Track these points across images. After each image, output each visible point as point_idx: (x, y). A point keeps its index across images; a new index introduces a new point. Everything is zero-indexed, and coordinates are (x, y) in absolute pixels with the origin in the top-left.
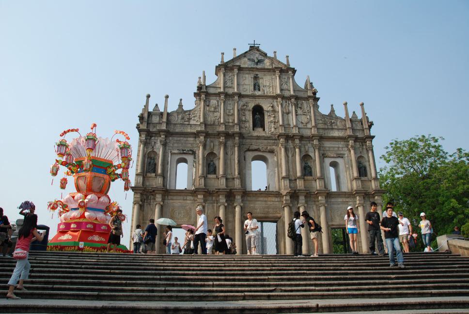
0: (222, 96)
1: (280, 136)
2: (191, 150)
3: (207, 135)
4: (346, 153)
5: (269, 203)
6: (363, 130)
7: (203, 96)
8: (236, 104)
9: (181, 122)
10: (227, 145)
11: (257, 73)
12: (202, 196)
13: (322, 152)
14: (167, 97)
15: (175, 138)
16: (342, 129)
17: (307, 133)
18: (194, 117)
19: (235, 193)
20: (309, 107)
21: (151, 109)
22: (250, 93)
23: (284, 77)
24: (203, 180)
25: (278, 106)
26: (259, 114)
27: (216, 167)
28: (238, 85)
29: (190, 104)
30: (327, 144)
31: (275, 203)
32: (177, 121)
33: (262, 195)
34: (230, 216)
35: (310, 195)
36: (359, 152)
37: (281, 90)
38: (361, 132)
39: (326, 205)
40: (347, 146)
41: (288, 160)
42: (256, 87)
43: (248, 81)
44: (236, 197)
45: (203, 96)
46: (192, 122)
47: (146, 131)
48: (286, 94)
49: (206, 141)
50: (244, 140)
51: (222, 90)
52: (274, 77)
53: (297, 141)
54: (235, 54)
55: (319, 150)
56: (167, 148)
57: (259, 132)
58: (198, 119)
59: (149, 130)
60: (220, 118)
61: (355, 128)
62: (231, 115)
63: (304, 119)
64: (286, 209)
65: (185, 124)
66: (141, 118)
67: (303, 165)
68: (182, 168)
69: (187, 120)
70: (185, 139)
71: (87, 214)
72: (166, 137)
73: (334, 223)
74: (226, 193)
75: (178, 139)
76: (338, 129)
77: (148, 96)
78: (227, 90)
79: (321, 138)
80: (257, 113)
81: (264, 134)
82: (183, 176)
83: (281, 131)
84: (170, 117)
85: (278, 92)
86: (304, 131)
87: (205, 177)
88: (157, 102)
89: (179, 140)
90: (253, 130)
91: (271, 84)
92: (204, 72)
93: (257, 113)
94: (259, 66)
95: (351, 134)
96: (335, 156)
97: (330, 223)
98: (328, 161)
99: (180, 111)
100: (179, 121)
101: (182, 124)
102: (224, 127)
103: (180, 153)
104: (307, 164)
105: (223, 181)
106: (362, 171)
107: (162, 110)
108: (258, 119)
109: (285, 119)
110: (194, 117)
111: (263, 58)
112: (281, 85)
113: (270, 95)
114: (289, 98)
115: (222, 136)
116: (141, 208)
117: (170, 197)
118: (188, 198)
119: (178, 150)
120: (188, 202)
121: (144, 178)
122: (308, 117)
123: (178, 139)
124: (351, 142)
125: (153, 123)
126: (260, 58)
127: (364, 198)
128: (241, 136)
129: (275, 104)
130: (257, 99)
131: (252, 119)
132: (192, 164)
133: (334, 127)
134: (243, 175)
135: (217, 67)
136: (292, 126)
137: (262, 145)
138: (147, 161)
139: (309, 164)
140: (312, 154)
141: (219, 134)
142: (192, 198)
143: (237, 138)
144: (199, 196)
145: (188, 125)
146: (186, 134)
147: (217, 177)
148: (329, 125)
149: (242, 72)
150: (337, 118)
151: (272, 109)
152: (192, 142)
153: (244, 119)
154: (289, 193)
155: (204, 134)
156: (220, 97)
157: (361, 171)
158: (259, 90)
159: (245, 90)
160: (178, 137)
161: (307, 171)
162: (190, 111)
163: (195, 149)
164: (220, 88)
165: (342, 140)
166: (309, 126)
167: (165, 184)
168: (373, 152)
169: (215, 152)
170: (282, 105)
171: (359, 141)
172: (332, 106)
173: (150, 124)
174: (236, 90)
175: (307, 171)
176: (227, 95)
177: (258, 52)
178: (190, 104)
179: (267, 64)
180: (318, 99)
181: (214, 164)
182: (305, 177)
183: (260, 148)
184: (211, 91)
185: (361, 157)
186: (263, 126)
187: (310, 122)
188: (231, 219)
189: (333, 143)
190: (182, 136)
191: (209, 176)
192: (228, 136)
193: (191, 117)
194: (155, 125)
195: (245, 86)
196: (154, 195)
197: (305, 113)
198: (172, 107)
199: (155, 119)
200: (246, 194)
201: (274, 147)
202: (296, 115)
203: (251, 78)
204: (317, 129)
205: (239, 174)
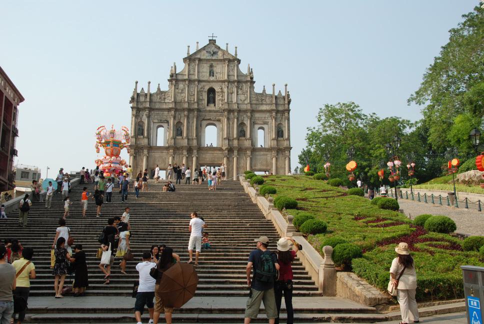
3: (176, 110)
4: (270, 121)
7: (174, 82)
11: (212, 62)
14: (149, 83)
17: (243, 107)
21: (139, 91)
24: (173, 140)
28: (198, 72)
29: (165, 87)
30: (257, 115)
34: (190, 163)
35: (241, 150)
36: (279, 121)
37: (228, 76)
38: (283, 106)
40: (271, 116)
41: (229, 127)
42: (212, 73)
43: (205, 68)
46: (166, 101)
48: (232, 79)
49: (175, 114)
50: (201, 113)
51: (186, 77)
53: (236, 114)
54: (197, 47)
55: (251, 119)
56: (150, 119)
57: (211, 107)
63: (242, 97)
64: (225, 159)
66: (133, 98)
67: (240, 129)
68: (161, 131)
71: (112, 165)
73: (256, 168)
76: (266, 104)
77: (137, 83)
79: (253, 111)
81: (214, 109)
82: (162, 137)
83: (226, 107)
84: (152, 97)
85: (226, 78)
87: (174, 138)
88: (143, 86)
90: (208, 105)
91: (221, 72)
92: (175, 63)
94: (214, 58)
95: (275, 108)
97: (254, 168)
98: (257, 126)
102: (187, 104)
103: (159, 122)
106: (280, 133)
107: (146, 92)
109: (230, 97)
111: (217, 50)
112: (228, 72)
114: (234, 82)
117: (153, 151)
118: (164, 151)
120: (164, 154)
121: (136, 138)
123: (158, 112)
124: (274, 114)
126: (216, 50)
128: (199, 110)
129: (223, 86)
134: (199, 137)
137: (212, 116)
139: (244, 129)
141: (184, 110)
142: (166, 152)
143: (196, 112)
144: (171, 151)
150: (267, 95)
152: (166, 115)
153: (201, 98)
158: (213, 76)
161: (242, 133)
162: (166, 92)
163: (168, 119)
164: (185, 75)
166: (246, 102)
170: (228, 87)
174: (196, 77)
175: (242, 133)
177: (214, 46)
178: (165, 87)
179: (220, 55)
180: (254, 82)
184: (180, 77)
185: (280, 124)
186: (214, 102)
188: (190, 165)
191: (178, 137)
192: (190, 110)
196: (143, 150)
198: (153, 90)
199: (142, 99)
200: (200, 149)
201: (221, 117)
202: (237, 94)
205: (197, 136)
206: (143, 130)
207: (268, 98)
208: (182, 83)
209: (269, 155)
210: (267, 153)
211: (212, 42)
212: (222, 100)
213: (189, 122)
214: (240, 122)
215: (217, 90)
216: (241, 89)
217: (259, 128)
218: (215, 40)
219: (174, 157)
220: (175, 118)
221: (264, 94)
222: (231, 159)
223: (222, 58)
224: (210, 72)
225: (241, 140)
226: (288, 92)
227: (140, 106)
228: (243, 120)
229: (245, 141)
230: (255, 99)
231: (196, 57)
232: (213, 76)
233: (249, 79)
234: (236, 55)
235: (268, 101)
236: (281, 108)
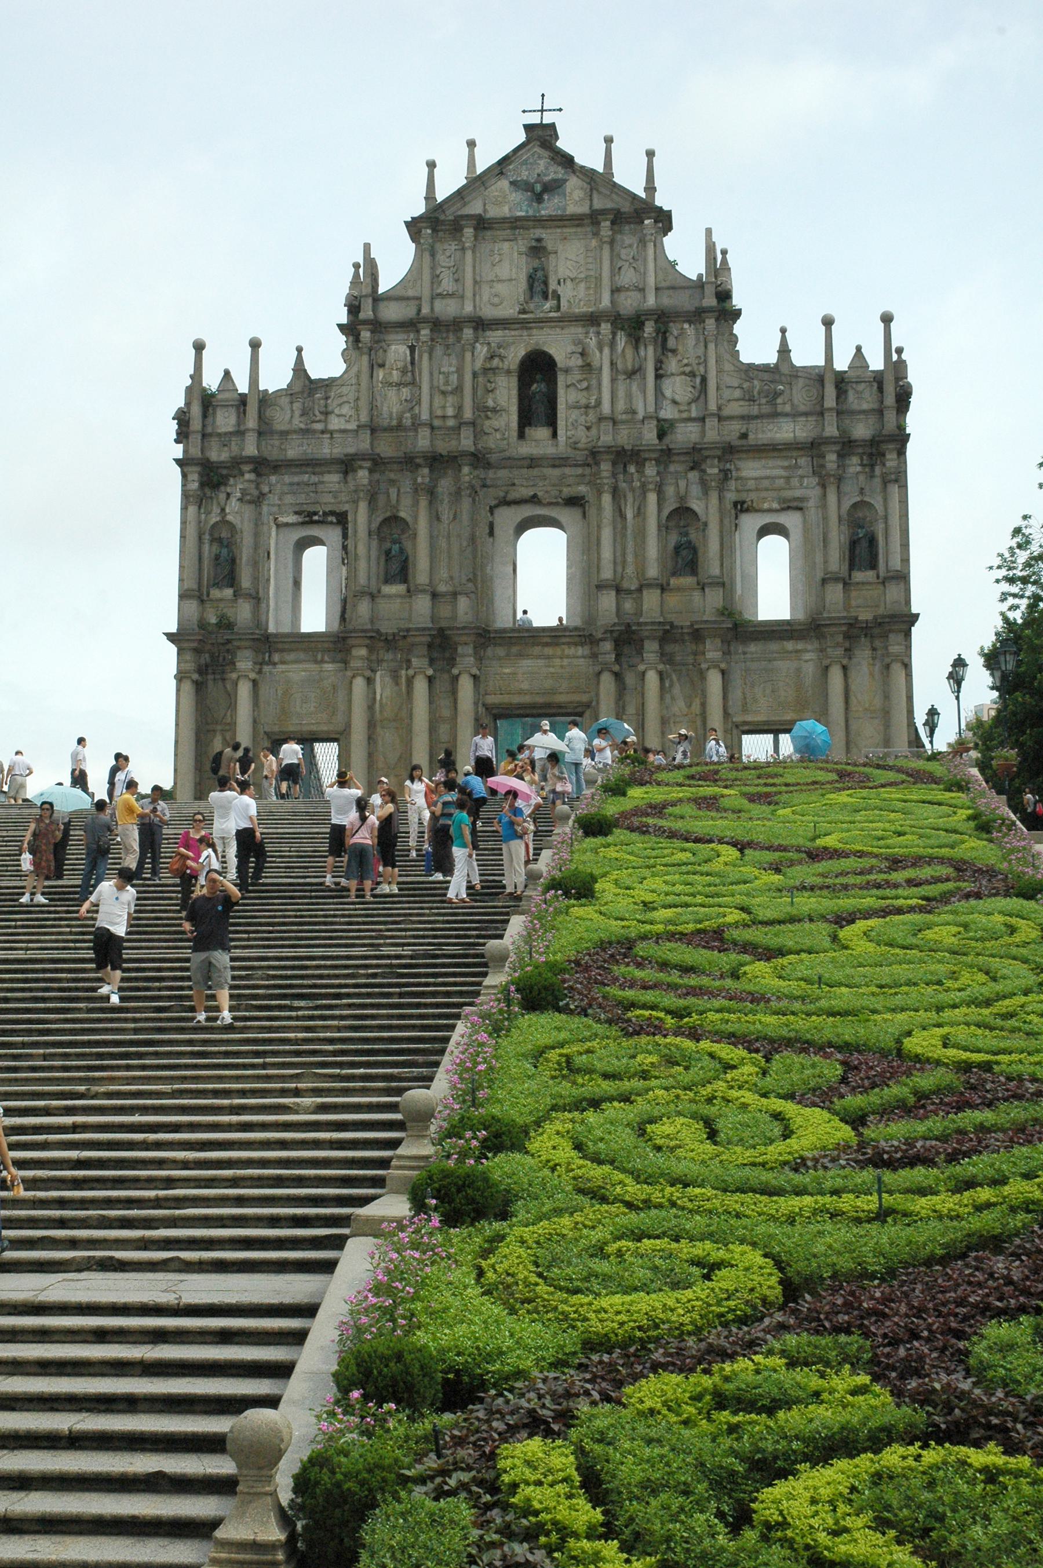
1: (594, 455)
2: (332, 513)
4: (815, 493)
5: (557, 662)
6: (880, 412)
8: (468, 355)
9: (302, 426)
10: (440, 490)
11: (539, 233)
12: (363, 652)
13: (731, 496)
14: (255, 345)
15: (287, 479)
16: (806, 414)
18: (340, 405)
19: (457, 639)
20: (702, 344)
23: (627, 242)
25: (601, 351)
26: (543, 380)
27: (407, 558)
28: (475, 282)
29: (328, 360)
30: (751, 469)
31: (575, 661)
32: (290, 422)
33: (564, 640)
37: (616, 290)
38: (872, 420)
39: (723, 666)
40: (818, 471)
41: (625, 528)
42: (538, 285)
44: (460, 650)
45: (366, 335)
47: (196, 464)
50: (491, 474)
51: (425, 310)
52: (594, 243)
53: (650, 470)
55: (721, 490)
56: (265, 509)
58: (352, 412)
59: (208, 460)
60: (419, 402)
61: (855, 407)
64: (607, 682)
65: (314, 431)
67: (673, 538)
69: (319, 417)
70: (315, 479)
72: (259, 475)
74: (429, 639)
75: (296, 479)
76: (795, 415)
77: (199, 347)
80: (538, 377)
83: (606, 439)
85: (606, 302)
89: (298, 484)
90: (521, 435)
92: (367, 247)
94: (550, 207)
96: (775, 506)
97: (738, 719)
98: (750, 523)
99: (297, 388)
100: (298, 423)
101: (306, 432)
103: (303, 523)
104: (687, 534)
105: (422, 605)
107: (243, 387)
109: (621, 394)
110: (340, 405)
112: (616, 271)
116: (199, 687)
119: (296, 513)
122: (698, 380)
123: (296, 479)
125: (219, 435)
127: (847, 636)
128: (479, 459)
129: (592, 342)
131: (515, 401)
132: (339, 553)
133: (779, 409)
135: (407, 224)
136: (640, 415)
138: (210, 551)
139: (693, 536)
140: (696, 505)
141: (409, 462)
145: (323, 432)
146: (320, 465)
147: (409, 591)
148: (763, 401)
149: (489, 233)
151: (580, 362)
153: (490, 403)
154: (612, 632)
155: (368, 464)
156: (418, 331)
157: (857, 552)
159: (496, 300)
160: (293, 474)
164: (419, 299)
165: (801, 453)
167: (263, 618)
168: (904, 487)
169: (402, 514)
171: (860, 450)
172: (783, 331)
173: (210, 435)
174: (468, 308)
176: (437, 324)
177: (546, 154)
178: (328, 360)
180: (737, 314)
181: (402, 550)
182: (674, 582)
183: (540, 494)
184: (391, 312)
186: (552, 422)
189: (771, 463)
190: (304, 469)
193: (330, 409)
194: (225, 439)
195: (499, 288)
198: (275, 378)
199: (225, 421)
202: (658, 377)
204: (720, 419)
206: (233, 561)
207: (801, 382)
208: (401, 336)
209: (808, 656)
210: (800, 646)
211: (541, 136)
212: (587, 407)
213: (438, 519)
214: (670, 506)
216: (674, 351)
217: (764, 531)
218: (552, 127)
219: (370, 681)
220: (372, 500)
221: (782, 370)
222: (630, 679)
223: (584, 209)
224: (531, 279)
225: (679, 589)
226: (899, 351)
227: (217, 454)
228: (682, 499)
229: (697, 595)
230: (737, 394)
231: (467, 211)
232: (545, 296)
234: (650, 188)
235: (800, 396)
236: (861, 431)
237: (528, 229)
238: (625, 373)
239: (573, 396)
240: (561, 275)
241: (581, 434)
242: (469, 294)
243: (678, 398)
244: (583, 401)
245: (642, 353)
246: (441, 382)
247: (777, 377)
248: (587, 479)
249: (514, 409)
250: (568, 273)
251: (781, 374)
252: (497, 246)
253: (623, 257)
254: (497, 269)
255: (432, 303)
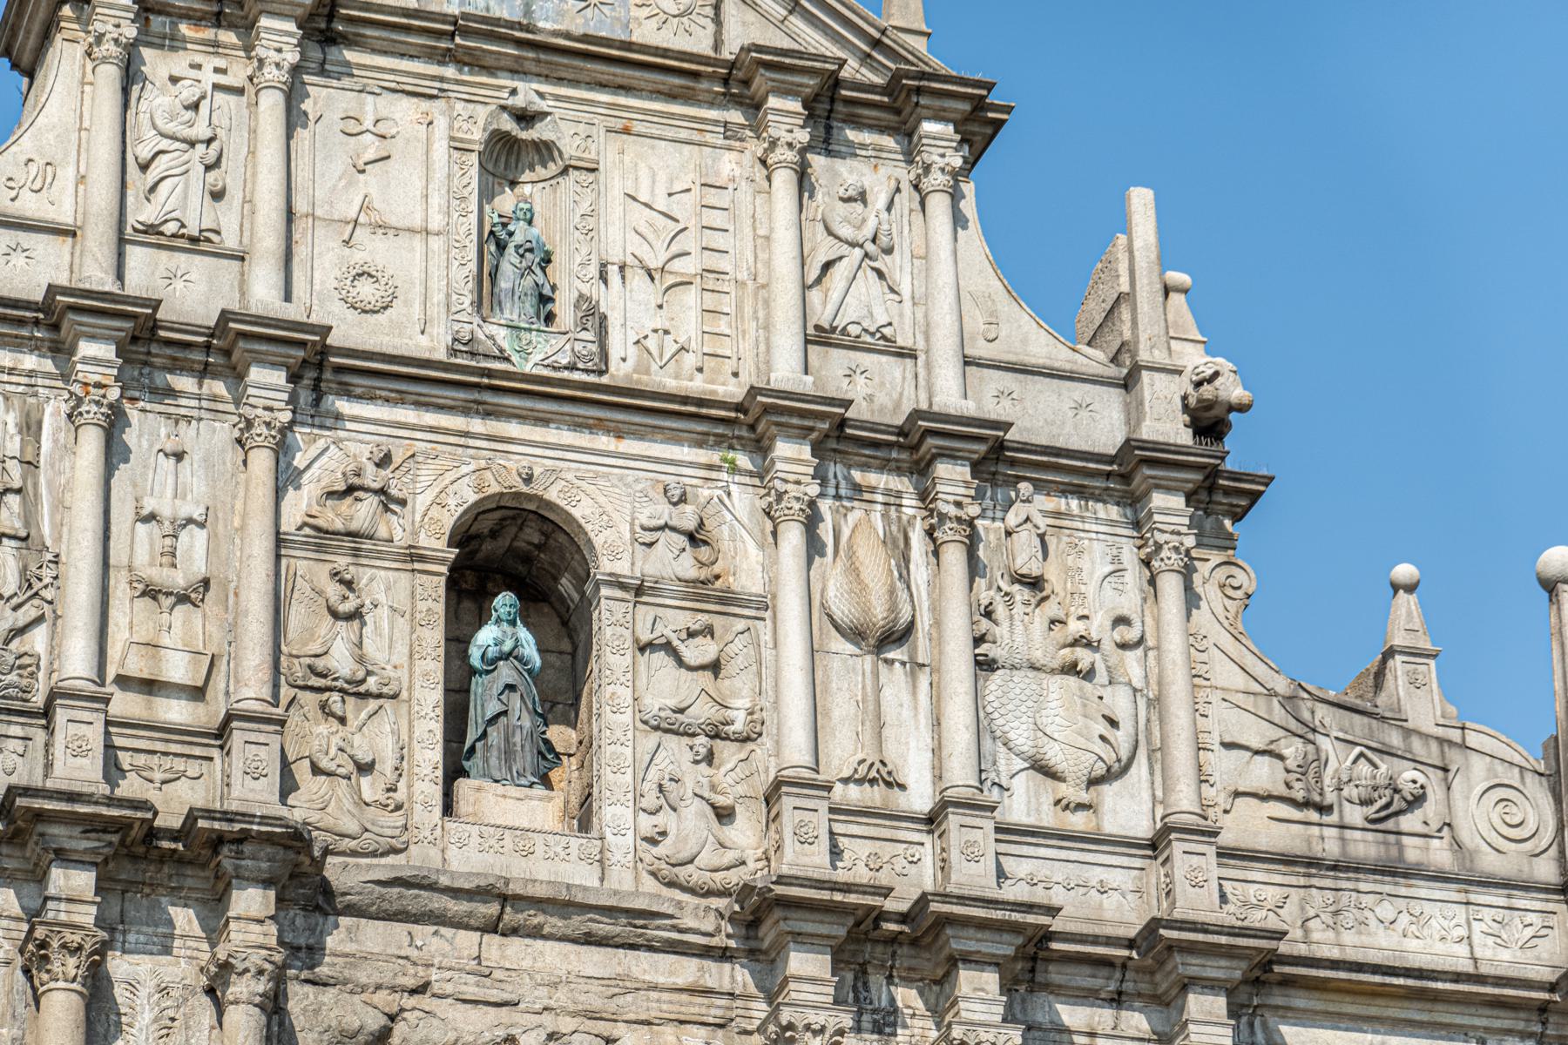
0: (86, 348)
11: (527, 93)
16: (1507, 885)
22: (433, 344)
52: (729, 165)
57: (508, 829)
60: (52, 616)
62: (183, 599)
78: (146, 272)
80: (504, 601)
86: (1059, 873)
93: (504, 601)
108: (506, 673)
109: (842, 707)
113: (671, 384)
114: (914, 445)
115: (63, 857)
130: (513, 429)
131: (432, 669)
133: (1413, 851)
136: (920, 799)
148: (1355, 815)
151: (687, 567)
153: (341, 662)
187: (1140, 769)
195: (373, 250)
197: (1084, 657)
203: (459, 146)
215: (614, 548)
230: (1264, 774)
233: (1185, 437)
237: (490, 70)
238: (855, 634)
239: (665, 687)
240: (615, 256)
241: (689, 827)
242: (268, 240)
243: (1055, 755)
244: (702, 712)
245: (920, 571)
246: (142, 557)
247: (1395, 739)
248: (715, 1009)
249: (430, 698)
250: (636, 246)
251: (1408, 733)
252: (370, 107)
253: (846, 231)
254: (370, 183)
255: (121, 255)
